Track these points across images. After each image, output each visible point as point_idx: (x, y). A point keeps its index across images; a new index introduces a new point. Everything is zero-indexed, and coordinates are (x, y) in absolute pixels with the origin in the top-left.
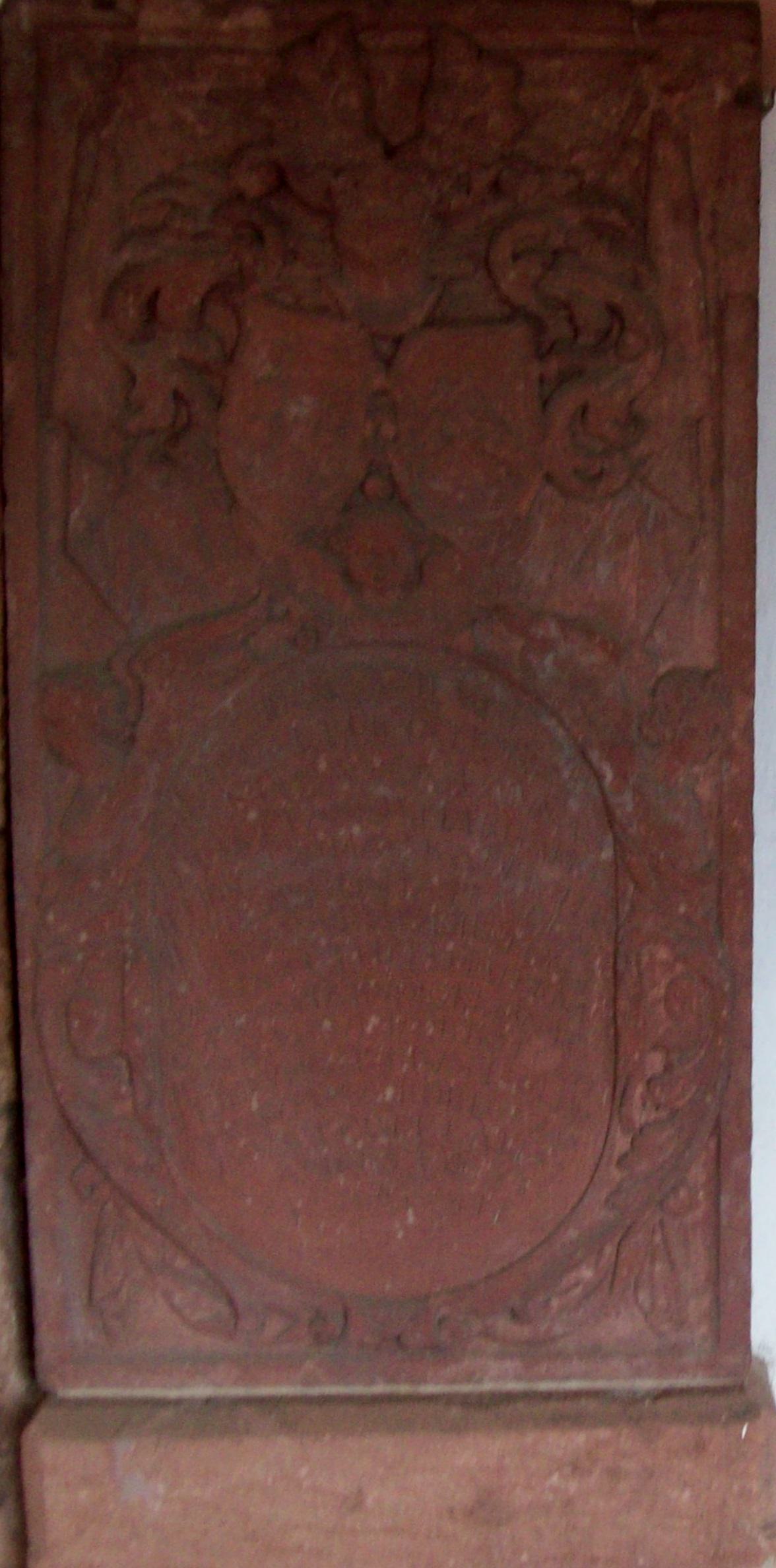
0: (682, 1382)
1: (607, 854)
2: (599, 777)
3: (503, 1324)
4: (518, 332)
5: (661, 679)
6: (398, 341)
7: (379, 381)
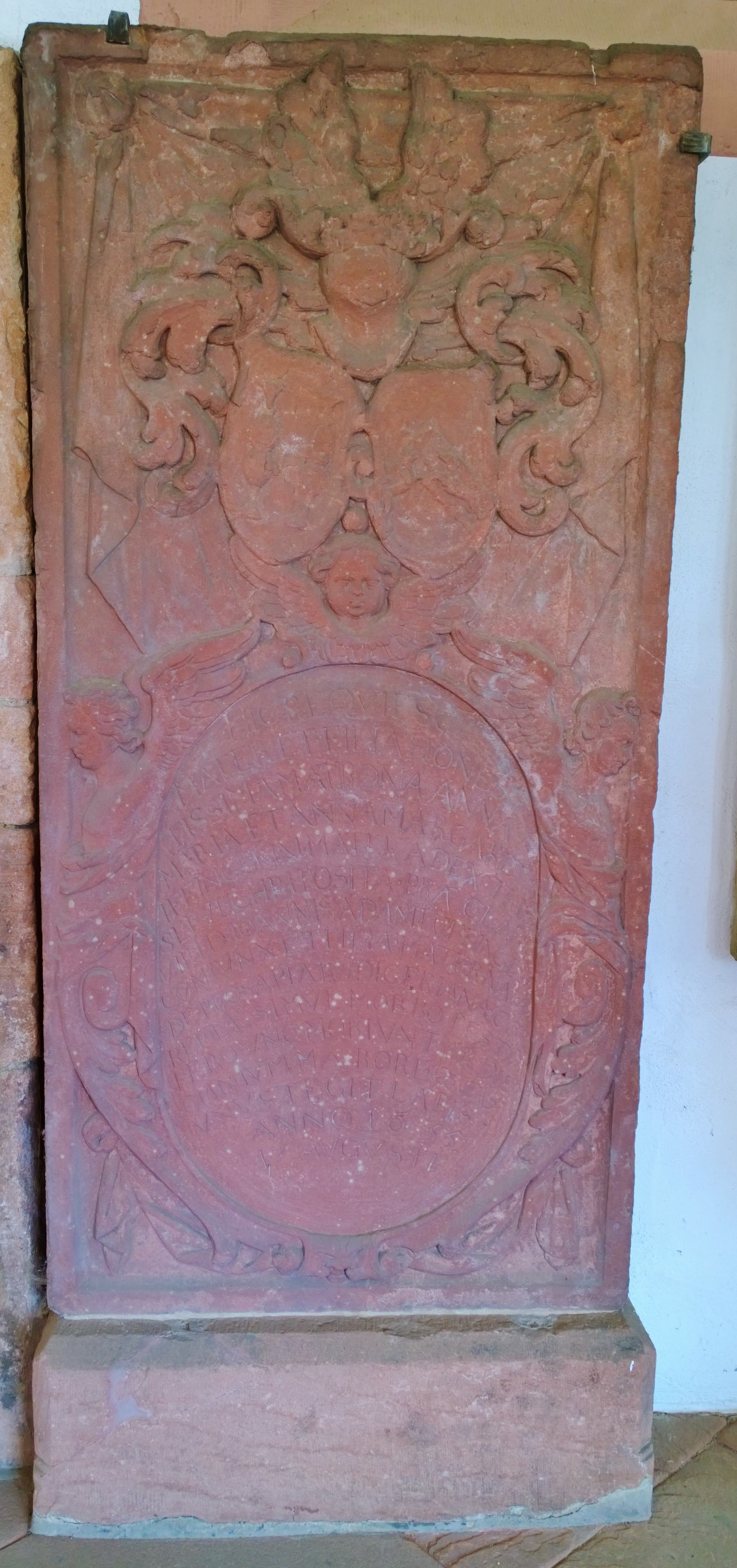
0: (573, 1311)
1: (533, 854)
2: (528, 784)
3: (430, 1258)
4: (480, 376)
5: (584, 699)
6: (376, 382)
7: (360, 422)
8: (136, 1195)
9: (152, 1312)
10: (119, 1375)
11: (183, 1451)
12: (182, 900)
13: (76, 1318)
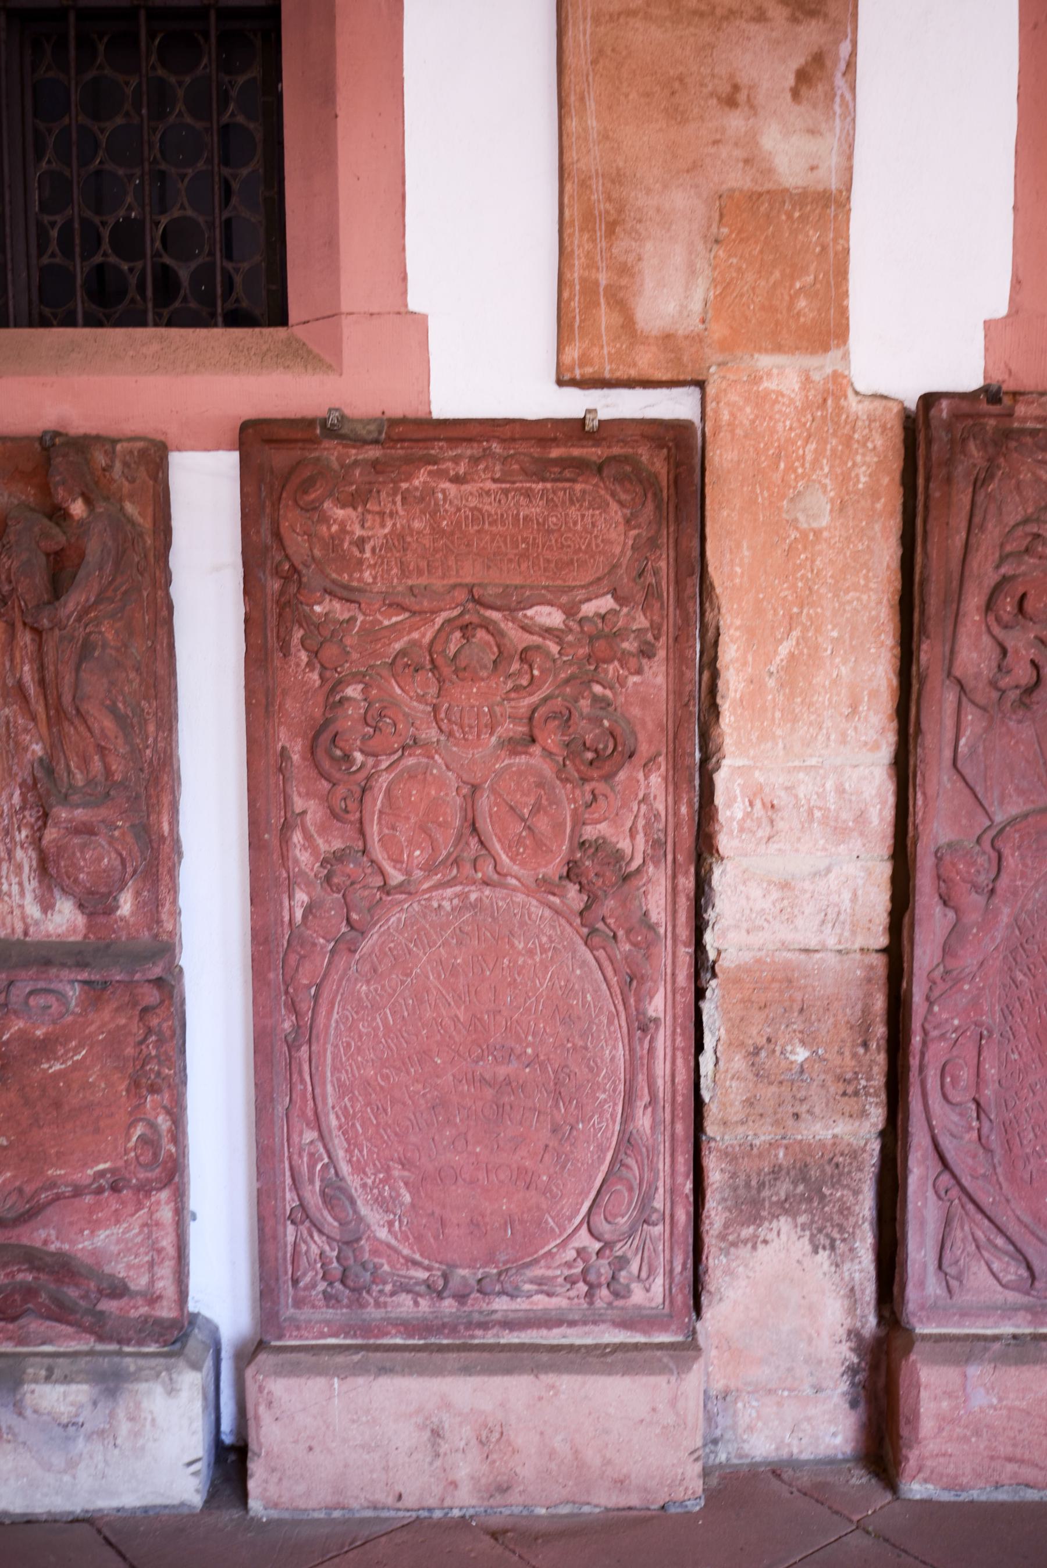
8: (973, 1234)
9: (984, 1327)
10: (973, 1371)
11: (1020, 1431)
12: (1017, 1004)
13: (927, 1331)
